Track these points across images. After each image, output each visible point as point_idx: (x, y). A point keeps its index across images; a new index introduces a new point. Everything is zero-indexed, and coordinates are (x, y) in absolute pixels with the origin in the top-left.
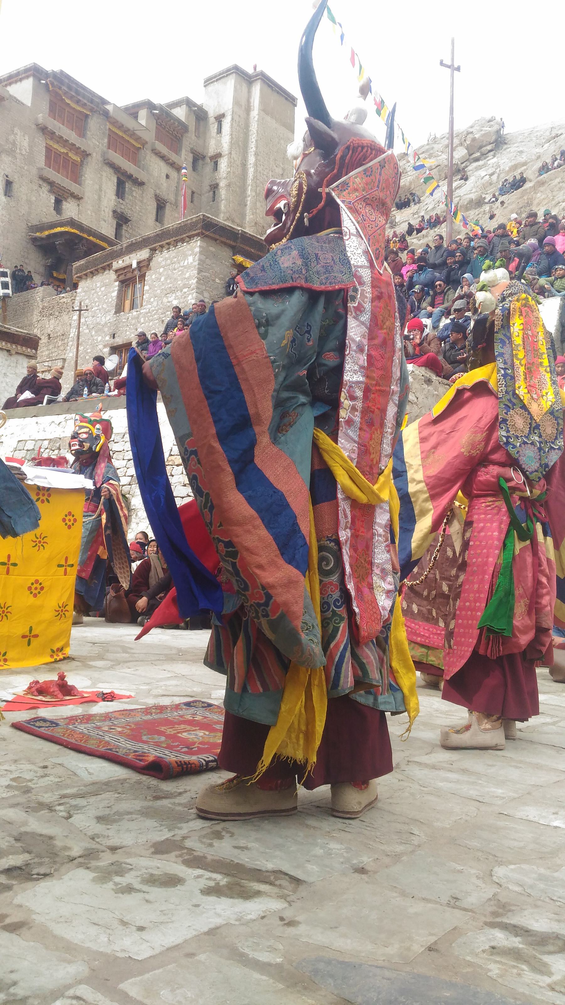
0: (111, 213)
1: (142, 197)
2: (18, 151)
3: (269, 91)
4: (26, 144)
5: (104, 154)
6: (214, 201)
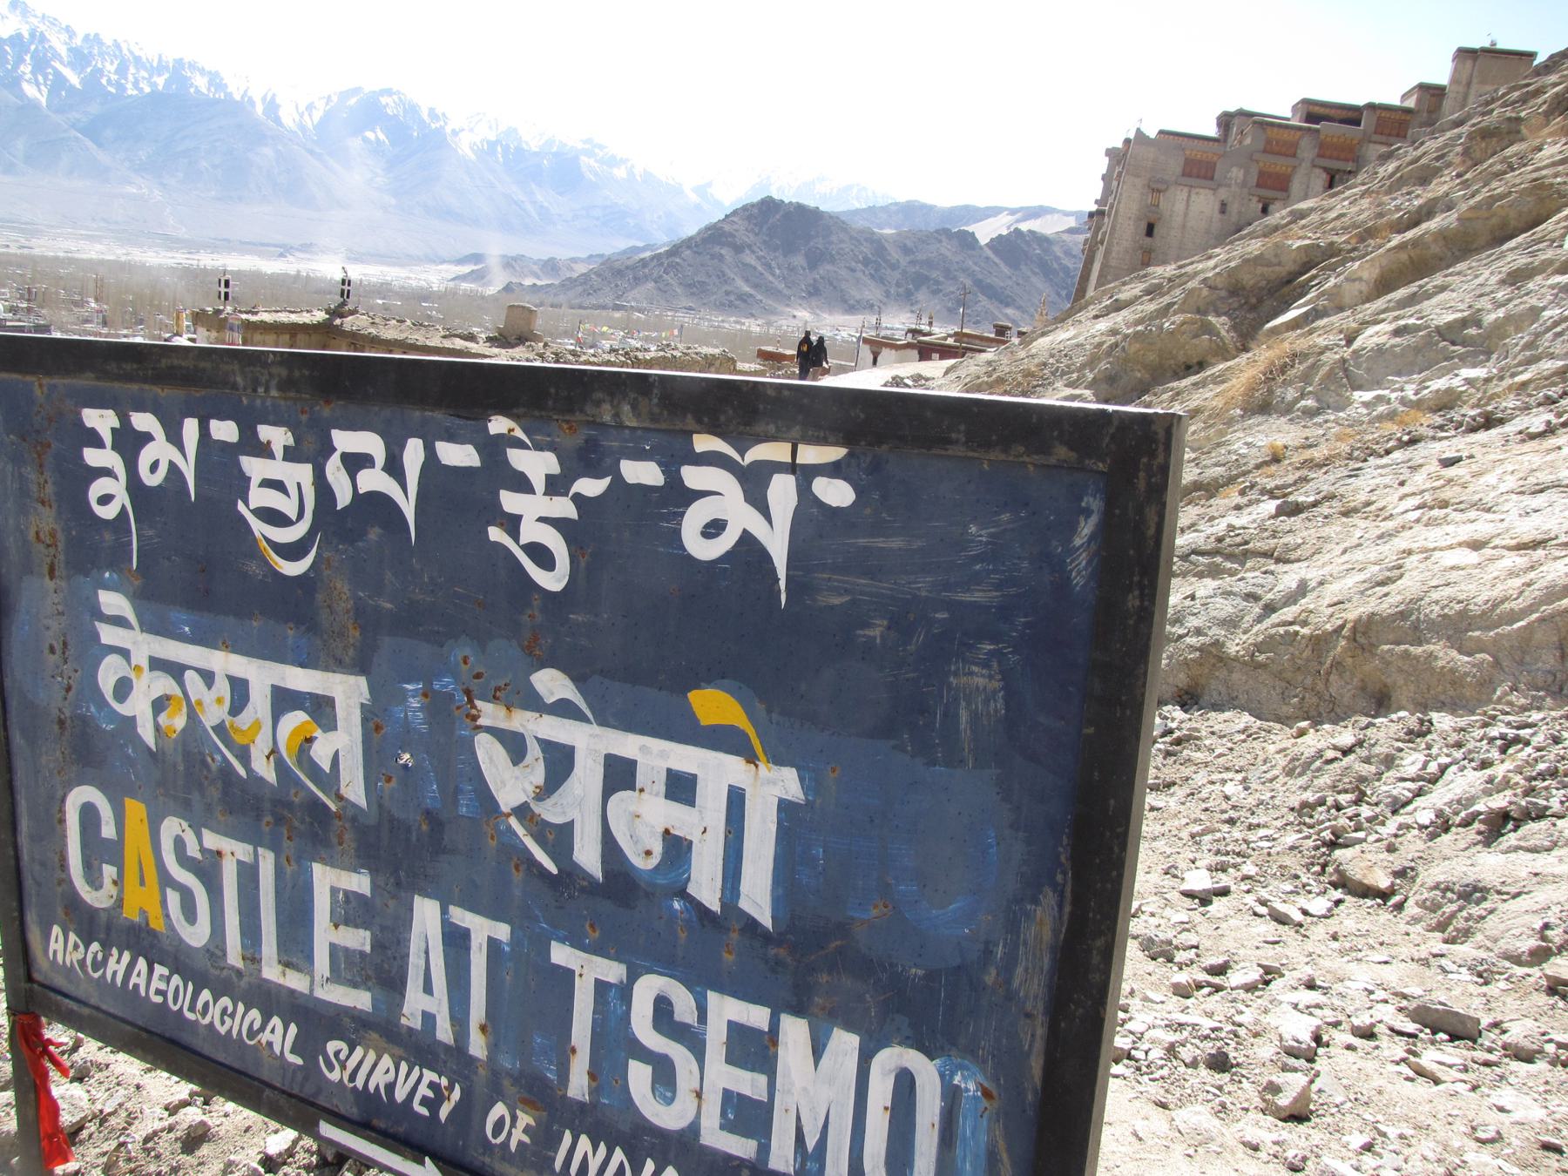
4: (1241, 174)
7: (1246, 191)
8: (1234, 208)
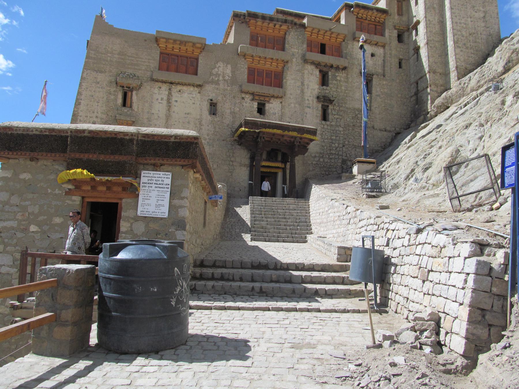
0: (315, 100)
4: (228, 71)
6: (417, 61)
7: (236, 88)
8: (225, 107)
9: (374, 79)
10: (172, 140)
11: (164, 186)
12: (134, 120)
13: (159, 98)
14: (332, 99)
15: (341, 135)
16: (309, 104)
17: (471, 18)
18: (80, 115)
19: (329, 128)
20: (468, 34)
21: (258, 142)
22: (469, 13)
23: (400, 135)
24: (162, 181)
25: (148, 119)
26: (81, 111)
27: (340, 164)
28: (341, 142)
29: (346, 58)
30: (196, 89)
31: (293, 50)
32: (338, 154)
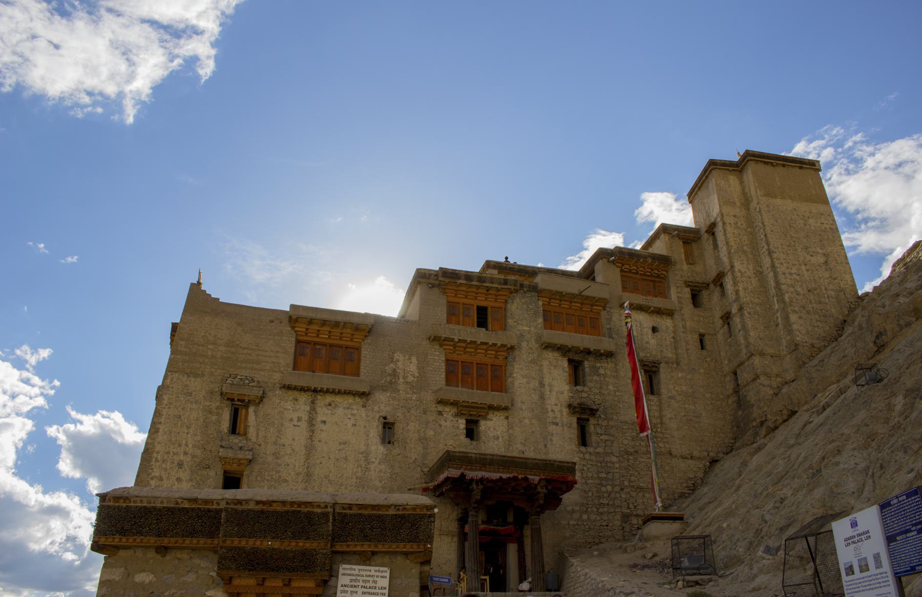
0: (565, 411)
1: (616, 371)
2: (401, 380)
3: (769, 168)
4: (413, 368)
5: (538, 338)
8: (409, 429)
9: (661, 370)
10: (392, 512)
11: (377, 591)
12: (250, 457)
13: (295, 416)
14: (594, 407)
15: (616, 471)
16: (555, 418)
17: (806, 265)
18: (156, 450)
19: (593, 458)
20: (805, 292)
21: (472, 490)
22: (801, 259)
23: (718, 465)
24: (375, 582)
25: (274, 454)
26: (159, 443)
27: (619, 523)
28: (617, 482)
29: (611, 337)
30: (358, 399)
31: (520, 327)
32: (613, 505)
